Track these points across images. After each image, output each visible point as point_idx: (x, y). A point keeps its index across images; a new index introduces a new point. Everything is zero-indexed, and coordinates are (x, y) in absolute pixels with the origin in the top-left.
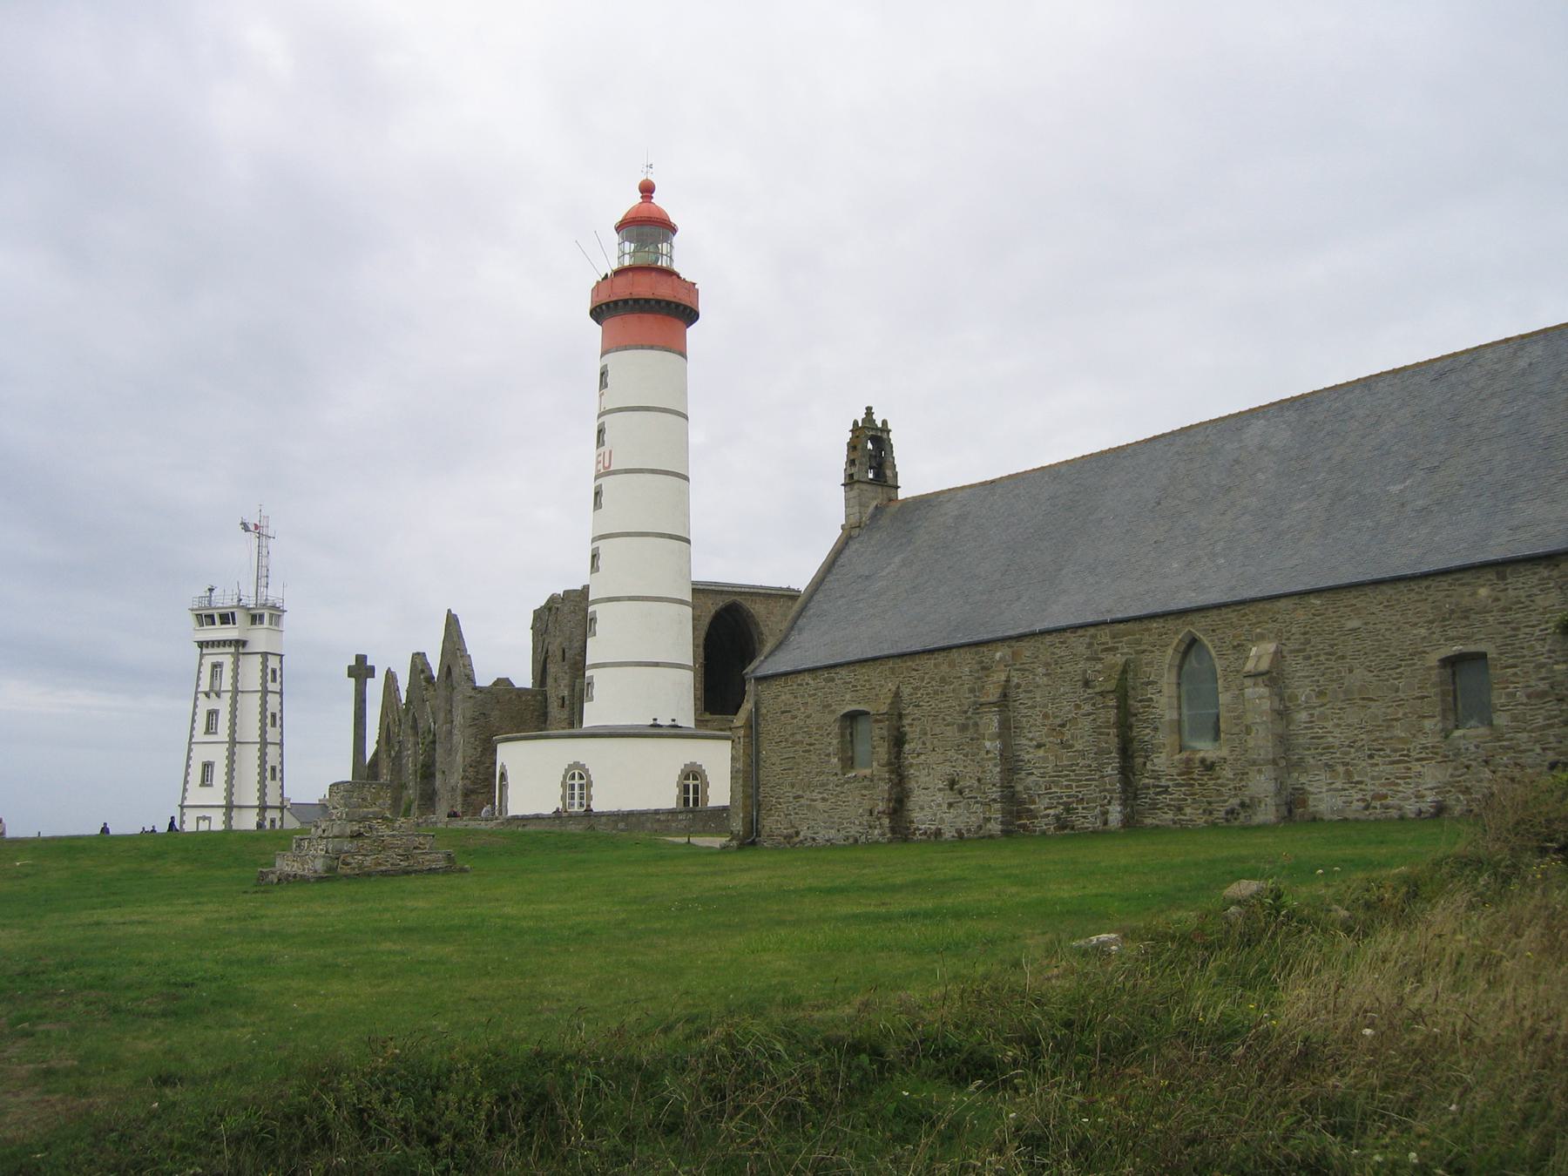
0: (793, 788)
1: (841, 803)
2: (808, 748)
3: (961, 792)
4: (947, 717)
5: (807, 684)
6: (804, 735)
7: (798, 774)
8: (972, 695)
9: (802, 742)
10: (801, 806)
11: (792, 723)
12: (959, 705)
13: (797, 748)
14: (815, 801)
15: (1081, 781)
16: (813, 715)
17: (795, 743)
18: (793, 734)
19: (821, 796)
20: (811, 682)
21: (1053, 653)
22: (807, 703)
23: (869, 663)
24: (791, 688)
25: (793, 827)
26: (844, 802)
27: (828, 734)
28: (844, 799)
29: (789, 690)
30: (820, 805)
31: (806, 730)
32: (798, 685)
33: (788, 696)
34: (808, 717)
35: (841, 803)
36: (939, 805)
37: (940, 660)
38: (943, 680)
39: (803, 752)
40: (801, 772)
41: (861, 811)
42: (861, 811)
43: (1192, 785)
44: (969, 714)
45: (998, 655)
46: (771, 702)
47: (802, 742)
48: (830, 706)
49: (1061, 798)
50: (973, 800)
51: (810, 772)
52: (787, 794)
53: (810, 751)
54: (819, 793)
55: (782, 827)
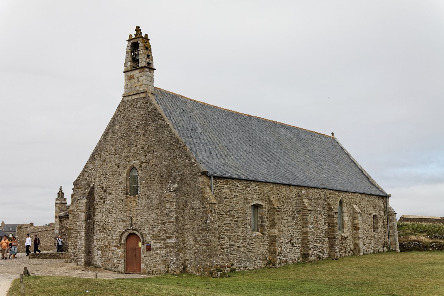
0: (230, 240)
1: (251, 248)
2: (237, 219)
3: (293, 244)
4: (289, 213)
5: (237, 186)
6: (235, 212)
7: (232, 233)
8: (296, 206)
9: (234, 216)
10: (234, 250)
11: (229, 205)
12: (292, 209)
13: (232, 218)
14: (240, 247)
15: (322, 241)
16: (240, 203)
17: (231, 216)
18: (229, 211)
19: (243, 245)
20: (239, 185)
21: (316, 195)
22: (237, 196)
23: (264, 183)
24: (229, 186)
25: (230, 261)
26: (252, 248)
27: (246, 213)
28: (252, 247)
29: (228, 187)
30: (242, 249)
31: (236, 210)
32: (233, 185)
33: (228, 190)
34: (237, 203)
35: (251, 248)
36: (286, 250)
37: (287, 189)
38: (288, 197)
39: (234, 221)
40: (233, 231)
41: (259, 252)
42: (259, 252)
43: (342, 244)
44: (295, 213)
45: (303, 192)
46: (218, 191)
47: (234, 216)
48: (247, 199)
49: (317, 247)
50: (296, 248)
51: (238, 232)
52: (226, 243)
53: (238, 221)
54: (242, 243)
55: (225, 262)
